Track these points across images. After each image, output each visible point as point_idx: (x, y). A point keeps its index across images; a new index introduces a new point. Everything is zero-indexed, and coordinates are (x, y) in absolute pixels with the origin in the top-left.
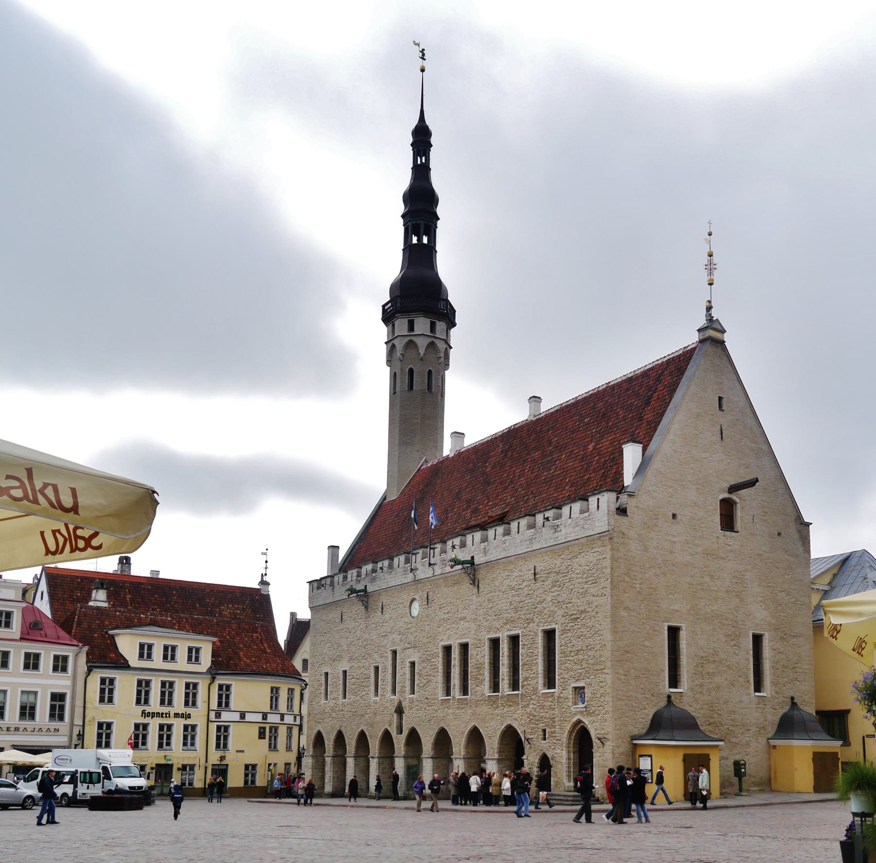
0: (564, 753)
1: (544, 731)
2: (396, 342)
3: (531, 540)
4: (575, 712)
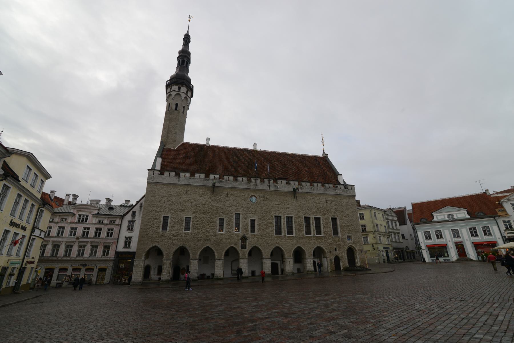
0: (346, 255)
1: (336, 249)
2: (180, 93)
3: (325, 190)
4: (349, 243)
